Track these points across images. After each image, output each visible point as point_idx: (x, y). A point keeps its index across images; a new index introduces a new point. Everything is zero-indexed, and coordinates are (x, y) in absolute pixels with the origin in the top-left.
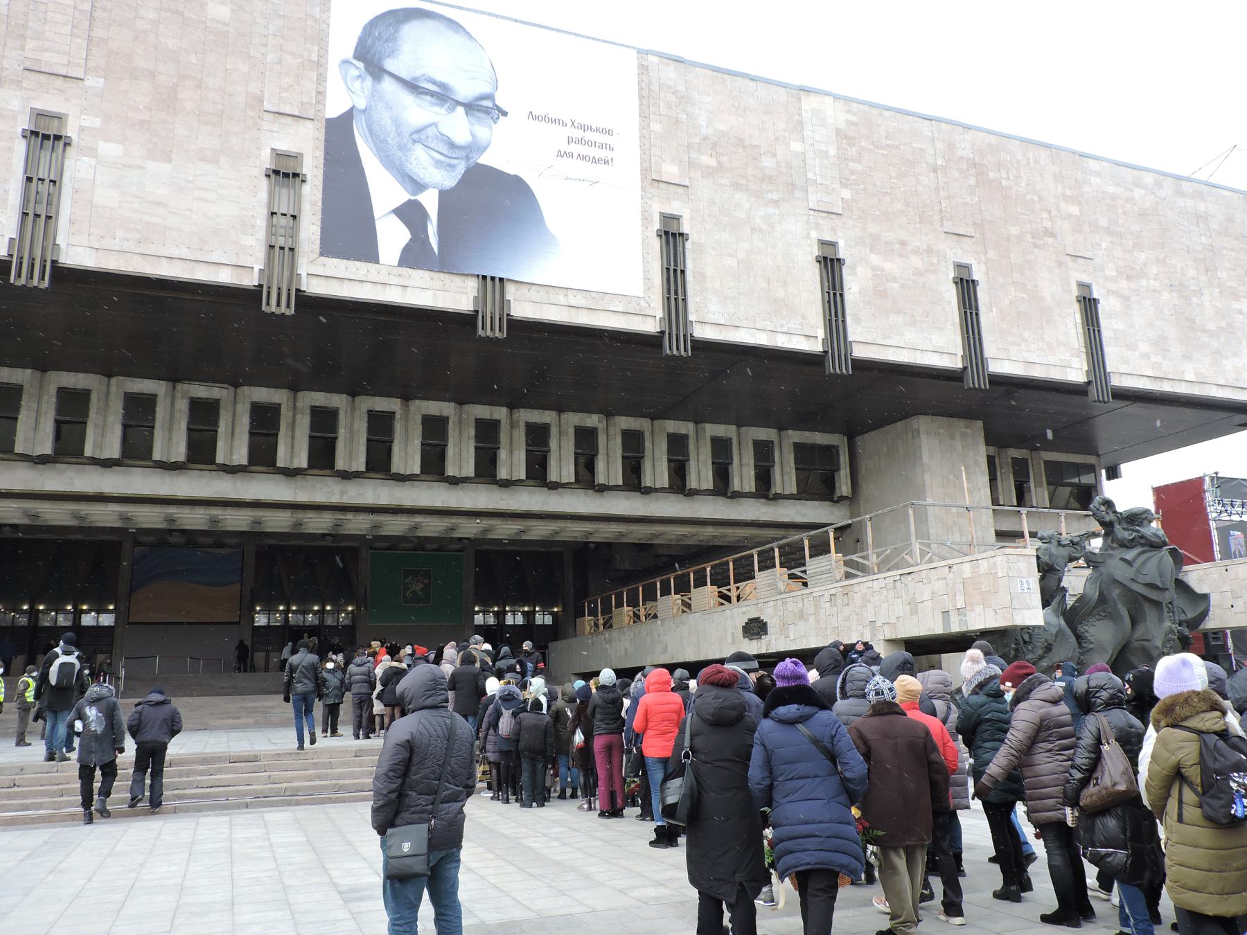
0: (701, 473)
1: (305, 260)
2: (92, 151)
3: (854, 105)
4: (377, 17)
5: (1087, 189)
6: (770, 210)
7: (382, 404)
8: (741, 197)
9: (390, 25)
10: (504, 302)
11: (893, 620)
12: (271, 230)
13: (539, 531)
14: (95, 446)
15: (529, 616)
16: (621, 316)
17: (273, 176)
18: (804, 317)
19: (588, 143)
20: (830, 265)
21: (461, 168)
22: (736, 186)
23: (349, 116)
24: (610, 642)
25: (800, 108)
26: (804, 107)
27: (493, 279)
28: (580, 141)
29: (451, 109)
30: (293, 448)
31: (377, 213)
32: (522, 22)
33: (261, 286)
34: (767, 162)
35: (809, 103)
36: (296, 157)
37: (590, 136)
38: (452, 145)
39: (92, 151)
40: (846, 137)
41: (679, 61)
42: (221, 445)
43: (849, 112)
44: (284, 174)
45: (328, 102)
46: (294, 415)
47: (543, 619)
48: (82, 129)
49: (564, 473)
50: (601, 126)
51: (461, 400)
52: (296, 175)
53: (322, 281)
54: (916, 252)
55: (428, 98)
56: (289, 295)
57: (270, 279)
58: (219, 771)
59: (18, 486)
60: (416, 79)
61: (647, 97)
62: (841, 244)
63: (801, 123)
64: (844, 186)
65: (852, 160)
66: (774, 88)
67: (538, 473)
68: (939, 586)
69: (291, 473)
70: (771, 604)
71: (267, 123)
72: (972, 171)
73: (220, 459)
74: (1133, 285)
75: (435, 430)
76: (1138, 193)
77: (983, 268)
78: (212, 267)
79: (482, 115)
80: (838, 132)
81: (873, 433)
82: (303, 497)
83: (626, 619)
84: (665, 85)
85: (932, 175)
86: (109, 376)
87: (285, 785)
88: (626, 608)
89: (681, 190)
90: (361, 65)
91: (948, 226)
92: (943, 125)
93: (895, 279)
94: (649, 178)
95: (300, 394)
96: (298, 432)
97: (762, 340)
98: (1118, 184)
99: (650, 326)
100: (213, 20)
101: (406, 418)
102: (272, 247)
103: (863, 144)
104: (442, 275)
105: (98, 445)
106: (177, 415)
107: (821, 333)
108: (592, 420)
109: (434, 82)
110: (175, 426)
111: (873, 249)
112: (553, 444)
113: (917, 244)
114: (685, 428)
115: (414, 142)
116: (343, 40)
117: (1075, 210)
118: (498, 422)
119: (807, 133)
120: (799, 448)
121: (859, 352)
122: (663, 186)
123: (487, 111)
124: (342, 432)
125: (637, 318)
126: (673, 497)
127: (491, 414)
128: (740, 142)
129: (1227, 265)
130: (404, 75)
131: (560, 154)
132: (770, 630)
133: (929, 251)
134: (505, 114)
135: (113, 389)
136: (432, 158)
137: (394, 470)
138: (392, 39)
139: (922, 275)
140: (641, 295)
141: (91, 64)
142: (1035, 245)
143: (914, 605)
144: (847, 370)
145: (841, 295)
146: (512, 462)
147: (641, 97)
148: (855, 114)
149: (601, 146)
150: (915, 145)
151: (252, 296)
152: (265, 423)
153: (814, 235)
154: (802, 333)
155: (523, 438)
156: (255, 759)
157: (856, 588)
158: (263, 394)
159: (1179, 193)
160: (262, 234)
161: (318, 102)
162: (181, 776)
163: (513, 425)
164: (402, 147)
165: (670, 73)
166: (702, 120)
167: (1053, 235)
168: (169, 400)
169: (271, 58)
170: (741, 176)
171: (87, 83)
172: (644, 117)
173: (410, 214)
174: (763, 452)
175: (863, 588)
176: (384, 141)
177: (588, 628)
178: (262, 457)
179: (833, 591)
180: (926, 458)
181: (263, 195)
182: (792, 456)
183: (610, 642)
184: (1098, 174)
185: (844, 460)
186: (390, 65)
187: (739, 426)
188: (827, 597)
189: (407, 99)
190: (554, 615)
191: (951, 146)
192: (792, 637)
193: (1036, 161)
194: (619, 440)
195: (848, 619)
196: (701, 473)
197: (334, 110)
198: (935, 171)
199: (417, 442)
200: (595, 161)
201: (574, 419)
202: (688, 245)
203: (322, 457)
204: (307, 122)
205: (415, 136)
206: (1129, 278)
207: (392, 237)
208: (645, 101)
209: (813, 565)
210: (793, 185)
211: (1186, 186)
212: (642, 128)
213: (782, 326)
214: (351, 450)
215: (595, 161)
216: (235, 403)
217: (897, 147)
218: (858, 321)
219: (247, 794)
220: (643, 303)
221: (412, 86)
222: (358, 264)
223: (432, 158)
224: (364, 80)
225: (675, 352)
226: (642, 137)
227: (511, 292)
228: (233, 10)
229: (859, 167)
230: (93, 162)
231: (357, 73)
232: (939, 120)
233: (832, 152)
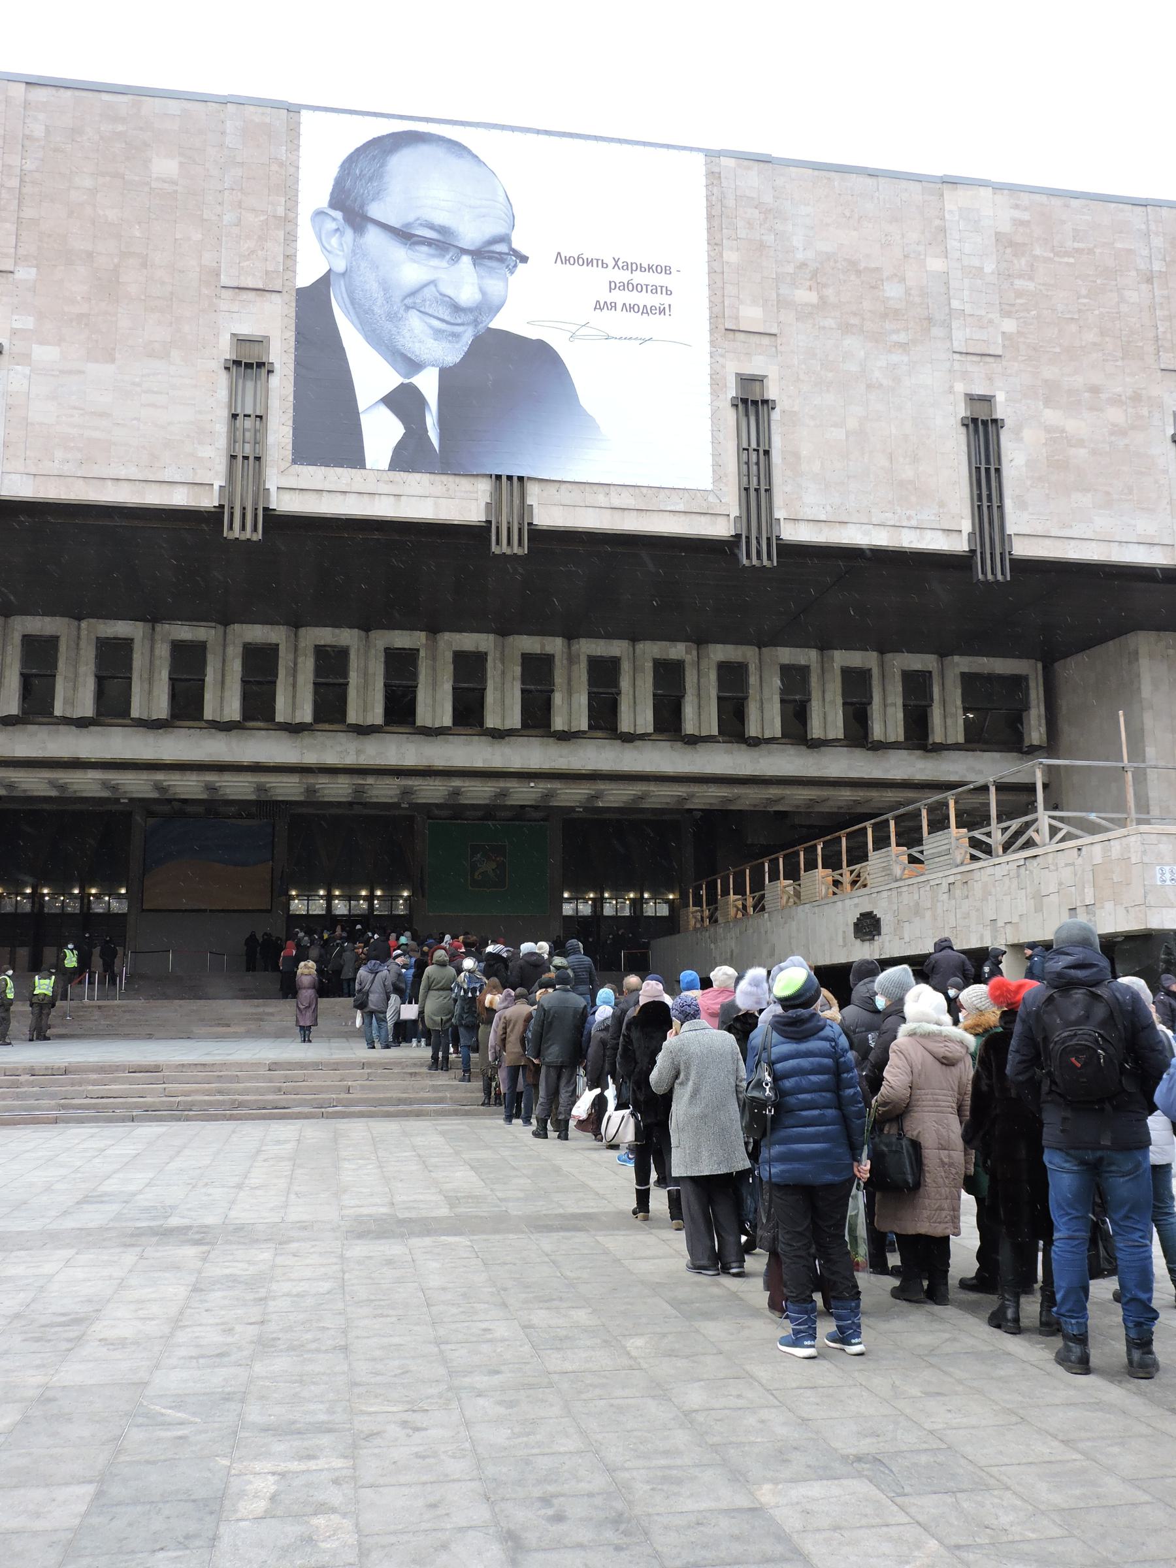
0: (828, 718)
1: (275, 470)
2: (25, 358)
3: (1025, 198)
4: (357, 150)
6: (895, 358)
7: (402, 639)
8: (851, 343)
9: (374, 158)
10: (525, 509)
11: (1015, 920)
12: (233, 439)
13: (617, 796)
14: (67, 702)
15: (637, 904)
16: (683, 517)
17: (234, 369)
18: (942, 504)
19: (636, 286)
20: (983, 429)
21: (468, 337)
23: (324, 282)
24: (715, 941)
25: (942, 209)
26: (948, 207)
27: (510, 478)
28: (625, 286)
29: (455, 260)
30: (295, 699)
31: (361, 408)
32: (547, 133)
33: (222, 506)
34: (893, 291)
35: (954, 201)
36: (261, 342)
37: (639, 278)
38: (456, 308)
39: (25, 358)
40: (1011, 244)
41: (764, 160)
42: (208, 696)
43: (1017, 207)
44: (248, 364)
45: (299, 268)
46: (296, 659)
47: (655, 909)
50: (654, 262)
51: (503, 632)
52: (260, 365)
53: (296, 496)
54: (1116, 401)
55: (425, 249)
56: (256, 515)
57: (231, 501)
58: (114, 1081)
60: (408, 225)
62: (1000, 397)
63: (943, 230)
64: (1006, 314)
65: (1020, 276)
66: (904, 184)
67: (604, 719)
68: (1066, 874)
69: (295, 729)
70: (885, 894)
71: (226, 302)
73: (208, 714)
78: (165, 487)
79: (494, 264)
81: (1083, 657)
82: (311, 758)
83: (732, 911)
84: (745, 194)
85: (1144, 287)
86: (79, 618)
87: (179, 1099)
88: (732, 897)
89: (766, 341)
90: (338, 215)
93: (1081, 443)
94: (721, 327)
95: (303, 631)
96: (301, 679)
97: (881, 539)
99: (721, 529)
100: (158, 179)
102: (233, 457)
103: (1038, 251)
104: (444, 478)
106: (157, 662)
107: (966, 526)
109: (431, 227)
110: (156, 675)
111: (1048, 402)
112: (625, 684)
113: (1119, 390)
114: (807, 657)
115: (408, 308)
116: (315, 187)
118: (553, 656)
119: (952, 244)
120: (969, 681)
121: (1022, 549)
122: (741, 336)
123: (500, 258)
124: (354, 678)
125: (703, 519)
126: (791, 750)
127: (543, 646)
131: (598, 306)
132: (885, 928)
133: (1136, 398)
134: (524, 259)
135: (84, 633)
136: (431, 327)
137: (419, 723)
138: (378, 175)
139: (1123, 433)
140: (710, 487)
141: (21, 251)
143: (1039, 898)
144: (1003, 575)
145: (998, 471)
146: (571, 707)
147: (710, 217)
148: (1026, 209)
149: (655, 290)
150: (1119, 245)
151: (213, 518)
152: (260, 666)
153: (960, 388)
155: (584, 677)
156: (156, 1069)
157: (976, 875)
158: (257, 633)
160: (222, 442)
161: (286, 269)
162: (73, 1085)
164: (392, 317)
165: (752, 180)
166: (797, 241)
168: (147, 644)
169: (227, 218)
170: (855, 314)
171: (17, 275)
172: (715, 244)
173: (404, 402)
174: (917, 687)
175: (984, 876)
176: (370, 311)
177: (692, 922)
178: (258, 709)
179: (951, 879)
180: (1146, 689)
181: (223, 394)
182: (959, 691)
183: (715, 941)
185: (1036, 695)
186: (375, 211)
187: (882, 652)
188: (945, 887)
189: (398, 252)
190: (671, 903)
192: (907, 939)
194: (713, 676)
195: (966, 916)
196: (828, 718)
197: (306, 277)
198: (1150, 280)
199: (447, 687)
200: (646, 311)
201: (652, 650)
202: (776, 415)
203: (330, 709)
204: (274, 295)
205: (409, 301)
207: (381, 433)
208: (716, 223)
209: (932, 843)
210: (929, 319)
212: (711, 260)
213: (909, 518)
214: (366, 700)
215: (646, 311)
216: (225, 646)
217: (1091, 251)
218: (1022, 505)
219: (137, 1106)
220: (712, 499)
221: (404, 236)
222: (339, 470)
223: (431, 327)
224: (342, 234)
225: (755, 562)
226: (712, 272)
227: (534, 495)
228: (181, 163)
229: (1031, 286)
230: (27, 370)
231: (333, 226)
232: (1158, 204)
233: (989, 267)
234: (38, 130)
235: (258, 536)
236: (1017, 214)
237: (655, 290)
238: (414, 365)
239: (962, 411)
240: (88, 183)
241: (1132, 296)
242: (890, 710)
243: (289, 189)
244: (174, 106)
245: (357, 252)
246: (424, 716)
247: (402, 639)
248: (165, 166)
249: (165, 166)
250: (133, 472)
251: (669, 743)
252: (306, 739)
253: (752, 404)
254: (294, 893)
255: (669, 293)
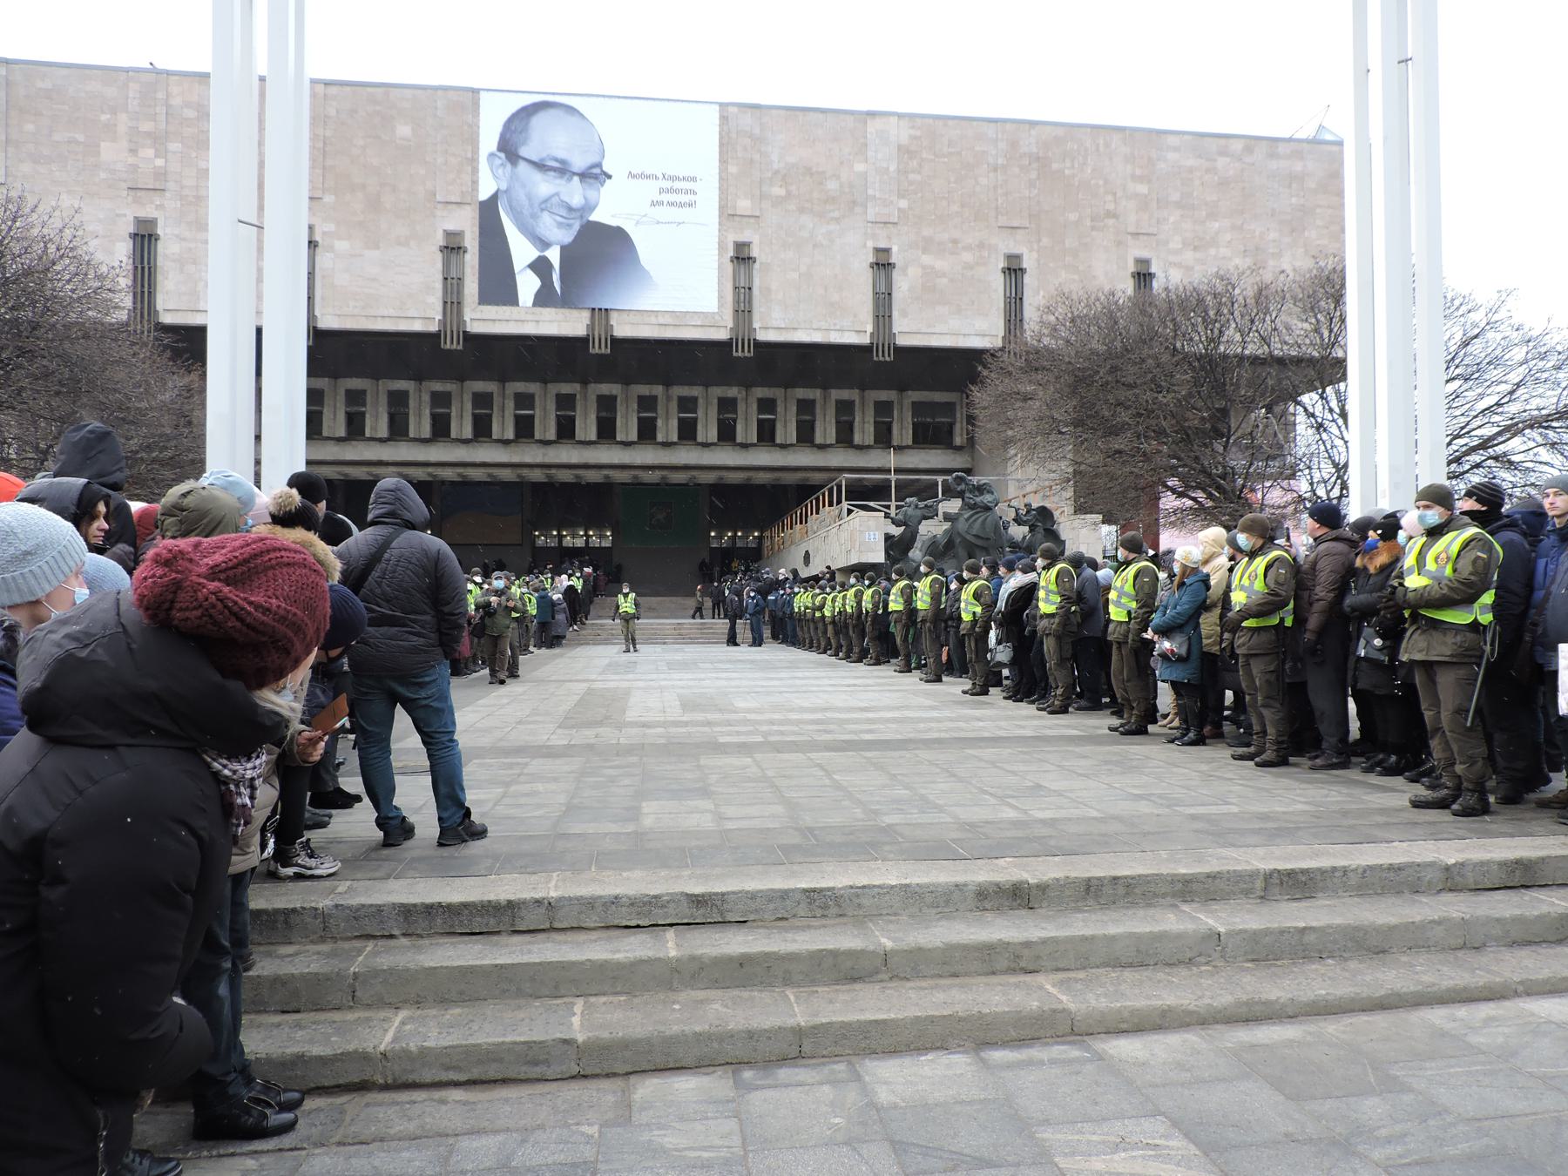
2: (331, 249)
3: (919, 121)
5: (1161, 165)
6: (833, 227)
7: (566, 388)
14: (374, 429)
19: (676, 191)
21: (577, 226)
22: (802, 210)
23: (494, 199)
28: (669, 191)
29: (570, 180)
31: (517, 268)
34: (832, 185)
35: (873, 126)
37: (678, 185)
38: (570, 209)
44: (452, 248)
48: (324, 233)
54: (968, 248)
59: (329, 458)
61: (726, 145)
62: (895, 249)
64: (901, 196)
72: (1035, 165)
73: (453, 435)
74: (1198, 255)
75: (607, 405)
76: (1222, 162)
77: (1035, 255)
80: (900, 147)
82: (516, 459)
84: (745, 131)
90: (502, 155)
91: (1003, 221)
92: (1008, 126)
93: (944, 275)
97: (817, 338)
98: (1200, 157)
99: (722, 335)
101: (585, 398)
105: (374, 429)
107: (870, 328)
108: (733, 392)
109: (556, 160)
116: (489, 140)
117: (1143, 189)
119: (870, 154)
120: (917, 407)
121: (902, 341)
123: (596, 177)
128: (809, 171)
129: (1319, 222)
130: (534, 158)
131: (653, 204)
133: (981, 246)
134: (610, 177)
138: (525, 129)
139: (971, 268)
142: (1093, 228)
147: (721, 145)
149: (687, 192)
153: (870, 244)
154: (853, 330)
158: (480, 386)
159: (1273, 155)
160: (439, 294)
163: (669, 398)
164: (534, 216)
165: (747, 120)
166: (775, 157)
167: (1115, 216)
172: (723, 161)
181: (439, 265)
184: (1176, 149)
189: (537, 176)
191: (1014, 144)
193: (1107, 145)
197: (484, 194)
198: (995, 170)
199: (593, 417)
200: (682, 205)
201: (718, 391)
202: (757, 266)
203: (524, 429)
206: (1195, 249)
207: (528, 284)
210: (854, 202)
211: (1281, 148)
214: (546, 427)
215: (682, 205)
218: (904, 314)
221: (540, 166)
226: (721, 179)
227: (614, 319)
229: (918, 177)
234: (332, 112)
235: (460, 347)
236: (912, 132)
237: (687, 192)
238: (544, 244)
239: (871, 259)
240: (361, 142)
241: (983, 181)
243: (473, 140)
244: (408, 93)
245: (513, 178)
247: (566, 388)
248: (404, 130)
249: (404, 130)
250: (392, 312)
252: (513, 447)
253: (742, 257)
255: (695, 193)
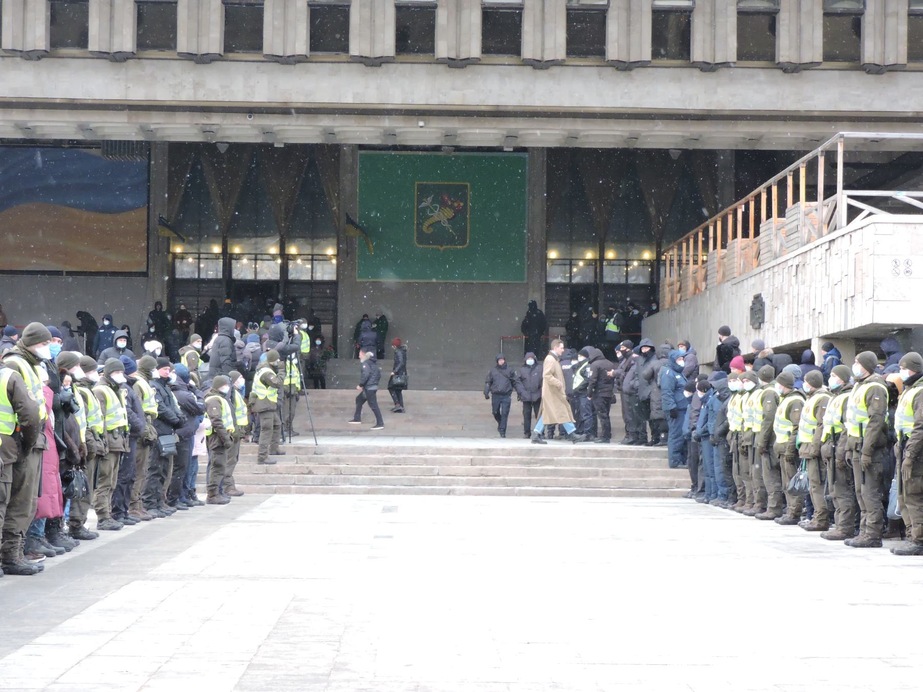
49: (549, 44)
82: (138, 94)
242: (891, 21)
246: (272, 42)
251: (594, 70)
254: (178, 249)
